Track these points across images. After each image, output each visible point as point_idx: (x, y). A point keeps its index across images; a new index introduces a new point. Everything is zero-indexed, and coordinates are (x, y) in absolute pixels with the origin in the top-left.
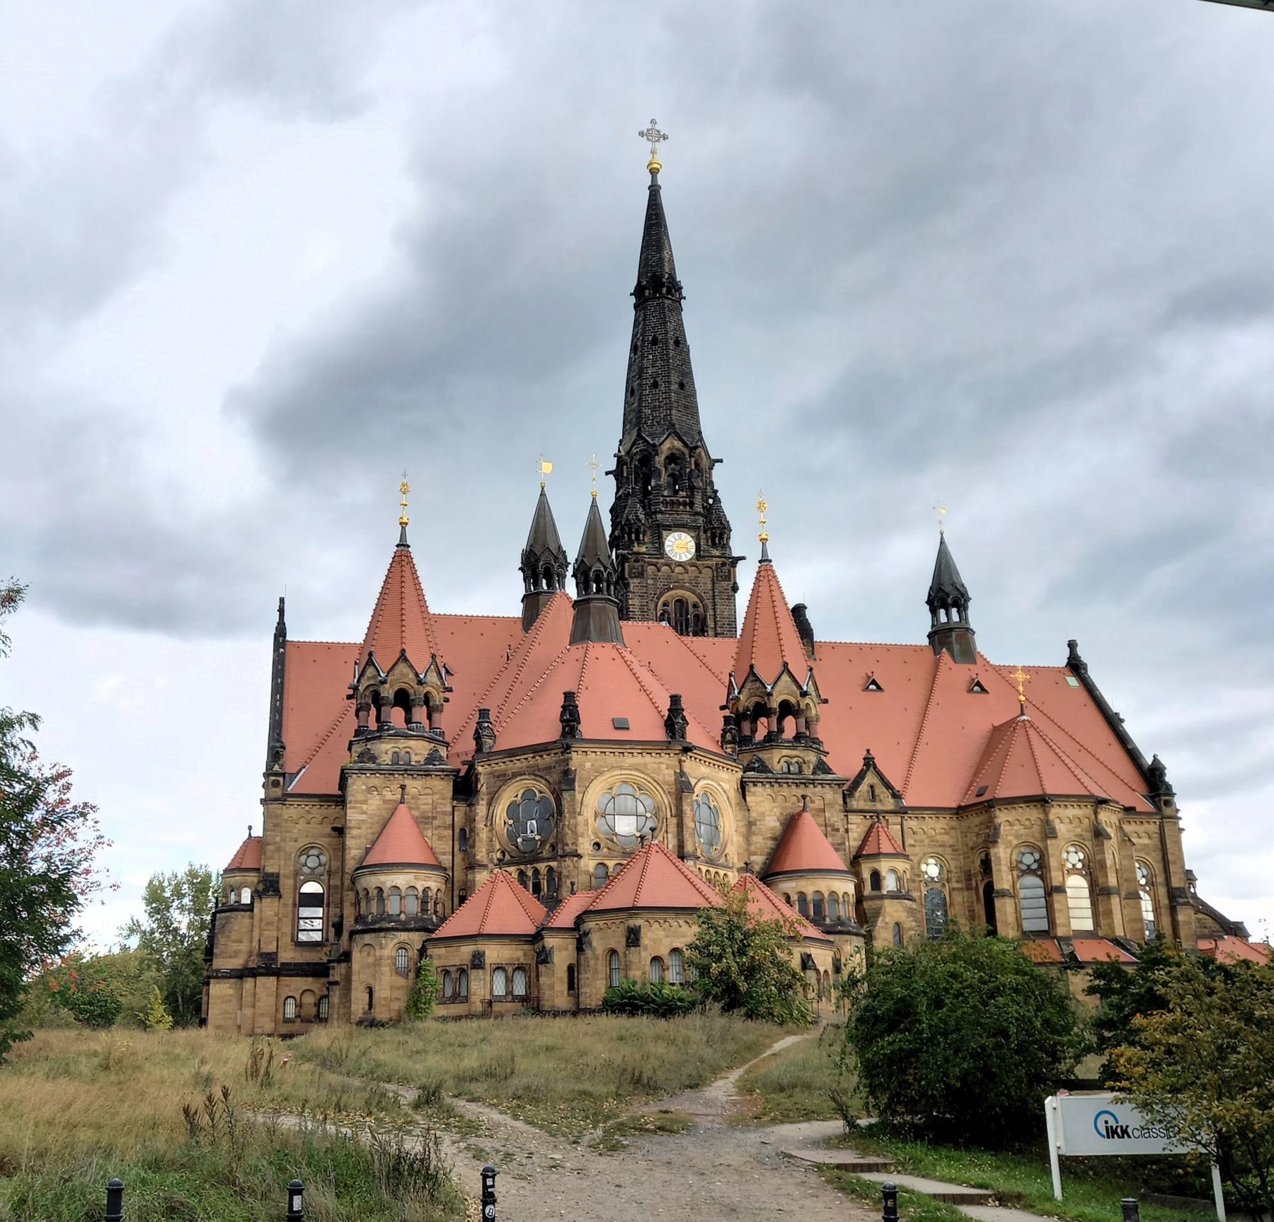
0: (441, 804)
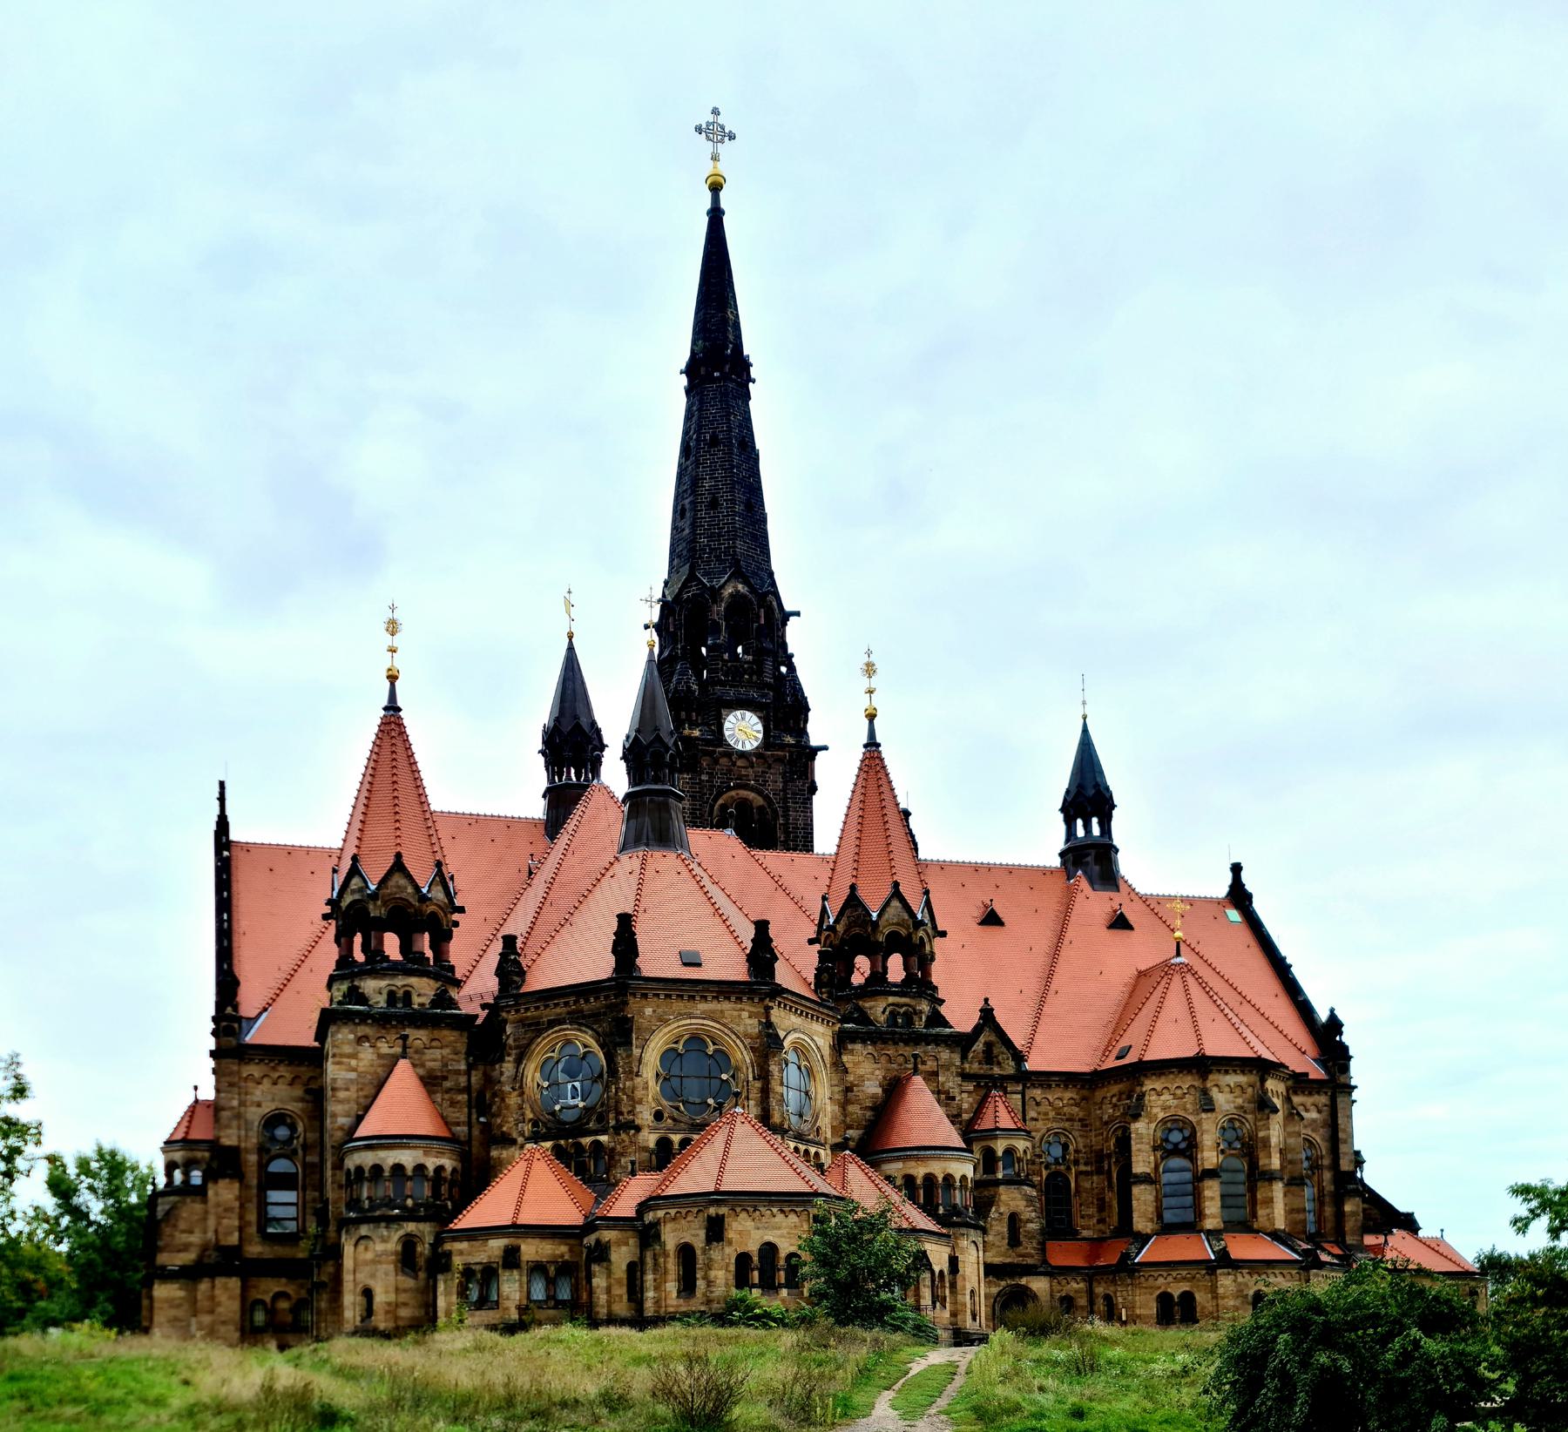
0: (454, 1060)
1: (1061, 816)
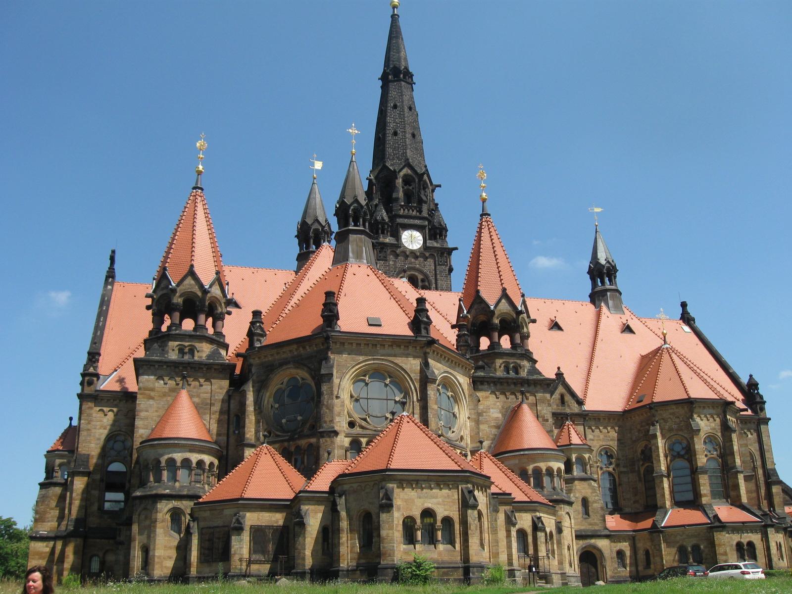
1: (588, 276)
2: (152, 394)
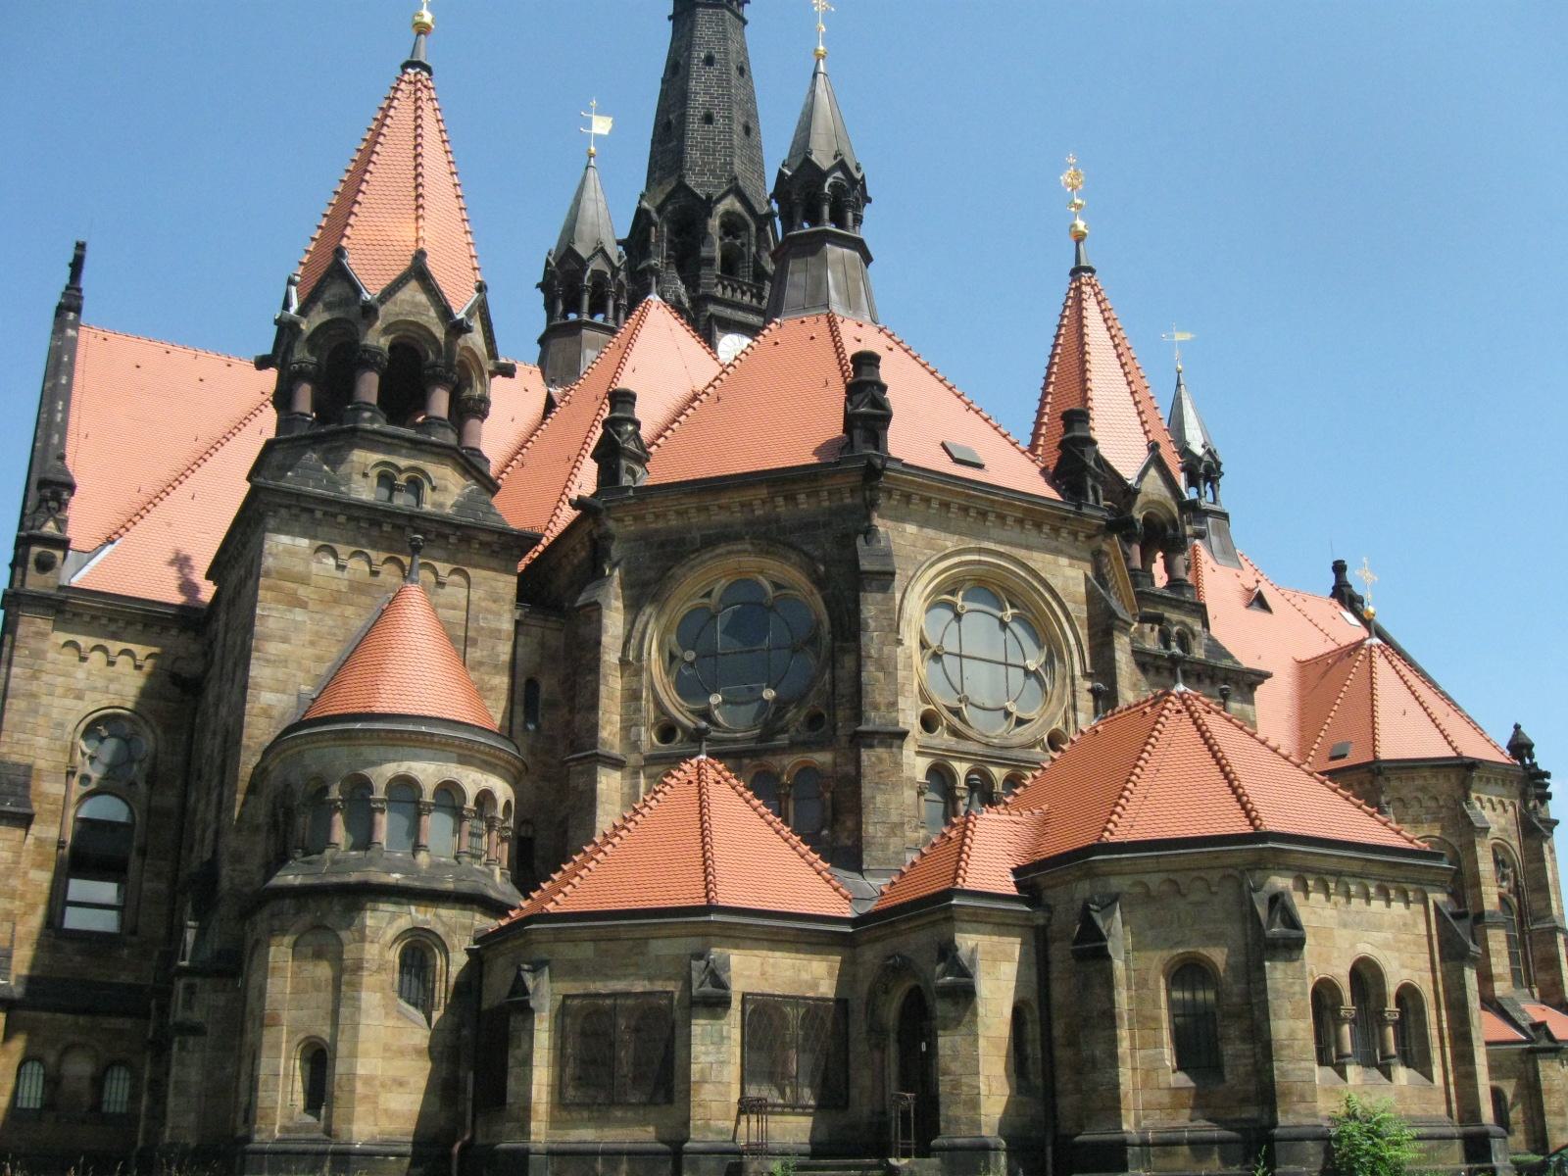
0: (488, 611)
2: (303, 592)
